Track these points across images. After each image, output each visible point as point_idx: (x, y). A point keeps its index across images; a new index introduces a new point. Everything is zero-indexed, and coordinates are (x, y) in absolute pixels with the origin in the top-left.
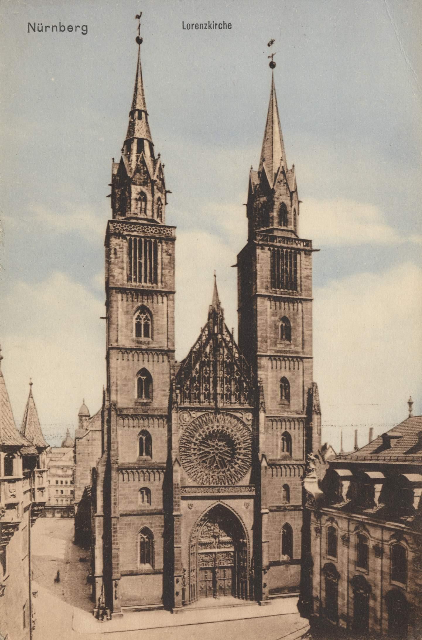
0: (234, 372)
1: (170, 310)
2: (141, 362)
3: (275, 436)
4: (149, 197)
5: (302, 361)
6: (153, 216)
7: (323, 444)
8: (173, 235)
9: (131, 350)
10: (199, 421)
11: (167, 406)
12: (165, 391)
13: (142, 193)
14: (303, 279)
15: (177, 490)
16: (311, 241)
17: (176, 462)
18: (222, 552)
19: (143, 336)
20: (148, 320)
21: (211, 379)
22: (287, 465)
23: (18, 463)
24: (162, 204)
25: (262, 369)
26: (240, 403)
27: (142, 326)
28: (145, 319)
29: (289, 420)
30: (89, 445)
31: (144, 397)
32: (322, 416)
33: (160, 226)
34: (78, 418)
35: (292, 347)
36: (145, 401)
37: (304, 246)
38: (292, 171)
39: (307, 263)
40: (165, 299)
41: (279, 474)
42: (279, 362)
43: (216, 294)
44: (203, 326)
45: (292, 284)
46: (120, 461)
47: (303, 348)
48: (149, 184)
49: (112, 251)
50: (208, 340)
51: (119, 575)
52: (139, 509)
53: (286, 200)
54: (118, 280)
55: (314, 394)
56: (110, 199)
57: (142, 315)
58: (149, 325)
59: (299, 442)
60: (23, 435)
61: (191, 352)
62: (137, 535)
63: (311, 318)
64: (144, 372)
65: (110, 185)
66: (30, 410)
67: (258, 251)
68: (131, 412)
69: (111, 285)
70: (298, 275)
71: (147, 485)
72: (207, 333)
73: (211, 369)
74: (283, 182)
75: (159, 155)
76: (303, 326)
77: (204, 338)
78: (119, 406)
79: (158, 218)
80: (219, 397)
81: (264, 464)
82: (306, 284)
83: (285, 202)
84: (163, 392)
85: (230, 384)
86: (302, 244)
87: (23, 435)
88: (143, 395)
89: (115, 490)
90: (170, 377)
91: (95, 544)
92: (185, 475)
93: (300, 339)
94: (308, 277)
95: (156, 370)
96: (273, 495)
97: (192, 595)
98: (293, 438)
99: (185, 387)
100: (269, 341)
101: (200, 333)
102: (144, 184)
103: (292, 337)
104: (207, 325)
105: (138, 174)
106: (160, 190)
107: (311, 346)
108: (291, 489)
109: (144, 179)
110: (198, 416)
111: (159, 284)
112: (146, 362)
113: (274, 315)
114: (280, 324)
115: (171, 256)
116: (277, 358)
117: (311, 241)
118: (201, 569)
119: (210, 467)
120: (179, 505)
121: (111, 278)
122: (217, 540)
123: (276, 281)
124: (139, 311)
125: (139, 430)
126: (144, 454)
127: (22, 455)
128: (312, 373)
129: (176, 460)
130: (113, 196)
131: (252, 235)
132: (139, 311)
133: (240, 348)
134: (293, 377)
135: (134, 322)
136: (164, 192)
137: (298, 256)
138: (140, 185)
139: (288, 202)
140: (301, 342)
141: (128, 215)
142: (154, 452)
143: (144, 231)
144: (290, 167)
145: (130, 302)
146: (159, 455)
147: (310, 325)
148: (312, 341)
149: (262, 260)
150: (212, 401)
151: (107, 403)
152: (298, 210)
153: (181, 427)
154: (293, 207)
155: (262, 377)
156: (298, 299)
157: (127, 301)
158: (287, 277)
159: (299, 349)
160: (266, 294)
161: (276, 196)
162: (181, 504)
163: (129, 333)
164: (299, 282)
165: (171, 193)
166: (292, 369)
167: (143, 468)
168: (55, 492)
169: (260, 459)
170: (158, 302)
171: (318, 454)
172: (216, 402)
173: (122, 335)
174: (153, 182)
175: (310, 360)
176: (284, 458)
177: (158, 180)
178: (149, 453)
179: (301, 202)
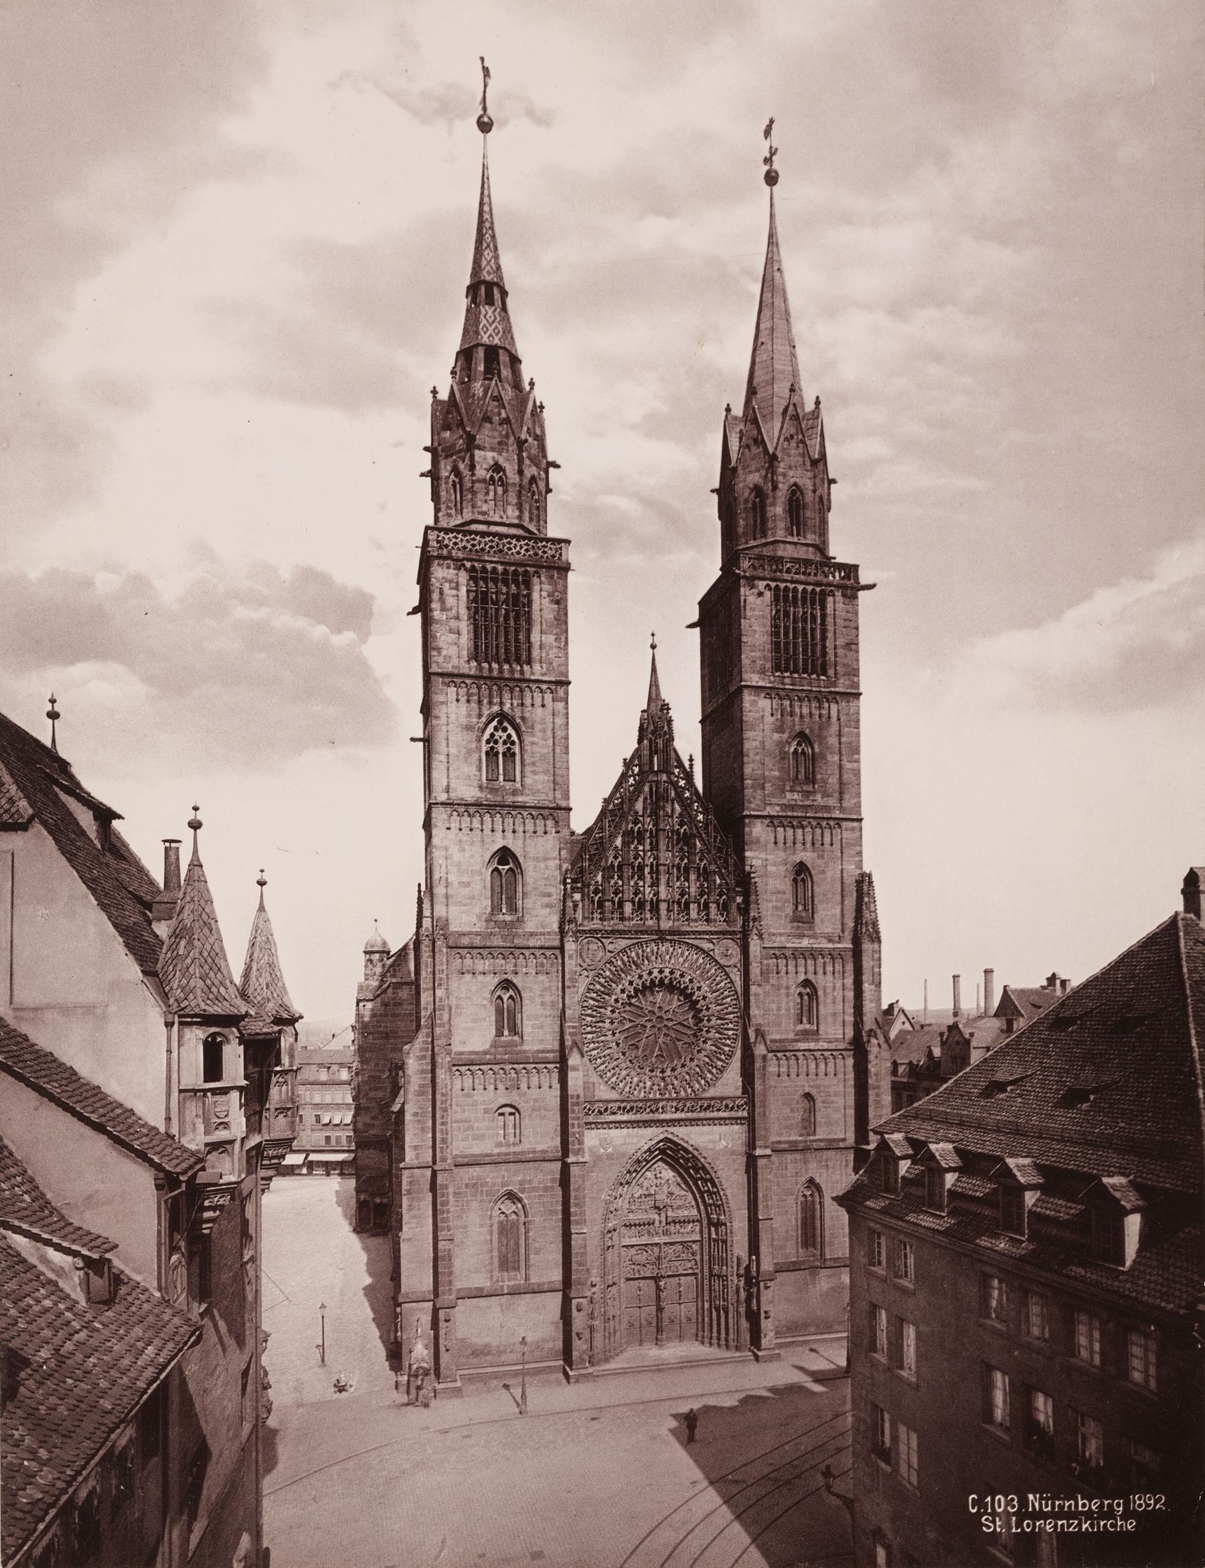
0: (695, 854)
2: (499, 834)
3: (783, 991)
5: (840, 827)
7: (885, 1006)
8: (564, 558)
9: (478, 804)
10: (622, 960)
11: (555, 927)
12: (550, 895)
13: (497, 468)
14: (839, 651)
15: (576, 1108)
16: (856, 567)
17: (575, 1050)
18: (672, 1244)
19: (501, 778)
20: (513, 743)
21: (647, 870)
22: (810, 1050)
23: (234, 1058)
24: (540, 493)
26: (707, 920)
27: (501, 756)
28: (505, 743)
29: (813, 954)
30: (386, 1015)
31: (504, 911)
32: (883, 944)
33: (538, 540)
34: (362, 958)
35: (819, 797)
36: (508, 918)
37: (842, 578)
38: (816, 414)
40: (548, 697)
41: (793, 1071)
42: (790, 832)
44: (628, 756)
45: (817, 664)
46: (457, 1047)
47: (841, 800)
48: (513, 447)
49: (435, 596)
51: (453, 1297)
52: (496, 1151)
54: (448, 658)
55: (866, 899)
58: (514, 754)
60: (243, 994)
61: (603, 814)
62: (492, 1208)
63: (858, 735)
64: (504, 855)
65: (426, 449)
66: (261, 943)
68: (477, 941)
69: (434, 668)
70: (829, 644)
71: (514, 1098)
72: (636, 770)
73: (648, 847)
74: (795, 440)
76: (840, 752)
78: (453, 928)
79: (531, 520)
80: (663, 907)
81: (760, 1050)
83: (800, 482)
84: (546, 900)
85: (687, 879)
86: (837, 574)
87: (243, 994)
88: (504, 906)
89: (445, 1110)
90: (560, 867)
91: (401, 1229)
92: (594, 1078)
93: (833, 780)
94: (852, 645)
95: (532, 851)
96: (780, 1121)
97: (609, 1335)
100: (767, 785)
101: (620, 769)
102: (501, 446)
103: (819, 777)
104: (637, 754)
105: (488, 425)
106: (535, 462)
107: (859, 795)
108: (819, 1104)
109: (501, 435)
110: (620, 948)
111: (537, 667)
113: (780, 729)
114: (792, 750)
115: (560, 602)
117: (856, 567)
118: (628, 1279)
119: (645, 1058)
120: (581, 1142)
121: (434, 653)
122: (663, 1218)
123: (782, 659)
124: (495, 723)
125: (496, 981)
126: (506, 1033)
127: (242, 1035)
128: (860, 853)
129: (575, 1043)
130: (433, 474)
131: (730, 557)
132: (495, 723)
134: (820, 862)
135: (485, 748)
136: (544, 465)
137: (830, 599)
138: (493, 449)
139: (806, 483)
140: (837, 787)
141: (468, 515)
143: (501, 551)
144: (809, 407)
145: (474, 705)
146: (538, 1032)
147: (857, 751)
148: (859, 784)
149: (753, 609)
150: (648, 915)
151: (427, 923)
152: (829, 501)
153: (586, 973)
154: (818, 493)
155: (754, 862)
156: (831, 692)
157: (468, 701)
159: (832, 802)
160: (761, 684)
161: (780, 470)
163: (473, 770)
164: (831, 656)
165: (558, 466)
166: (818, 844)
167: (506, 1059)
168: (314, 1119)
169: (752, 1040)
171: (874, 1027)
172: (658, 919)
174: (521, 444)
175: (856, 824)
177: (530, 440)
178: (514, 1030)
179: (834, 481)
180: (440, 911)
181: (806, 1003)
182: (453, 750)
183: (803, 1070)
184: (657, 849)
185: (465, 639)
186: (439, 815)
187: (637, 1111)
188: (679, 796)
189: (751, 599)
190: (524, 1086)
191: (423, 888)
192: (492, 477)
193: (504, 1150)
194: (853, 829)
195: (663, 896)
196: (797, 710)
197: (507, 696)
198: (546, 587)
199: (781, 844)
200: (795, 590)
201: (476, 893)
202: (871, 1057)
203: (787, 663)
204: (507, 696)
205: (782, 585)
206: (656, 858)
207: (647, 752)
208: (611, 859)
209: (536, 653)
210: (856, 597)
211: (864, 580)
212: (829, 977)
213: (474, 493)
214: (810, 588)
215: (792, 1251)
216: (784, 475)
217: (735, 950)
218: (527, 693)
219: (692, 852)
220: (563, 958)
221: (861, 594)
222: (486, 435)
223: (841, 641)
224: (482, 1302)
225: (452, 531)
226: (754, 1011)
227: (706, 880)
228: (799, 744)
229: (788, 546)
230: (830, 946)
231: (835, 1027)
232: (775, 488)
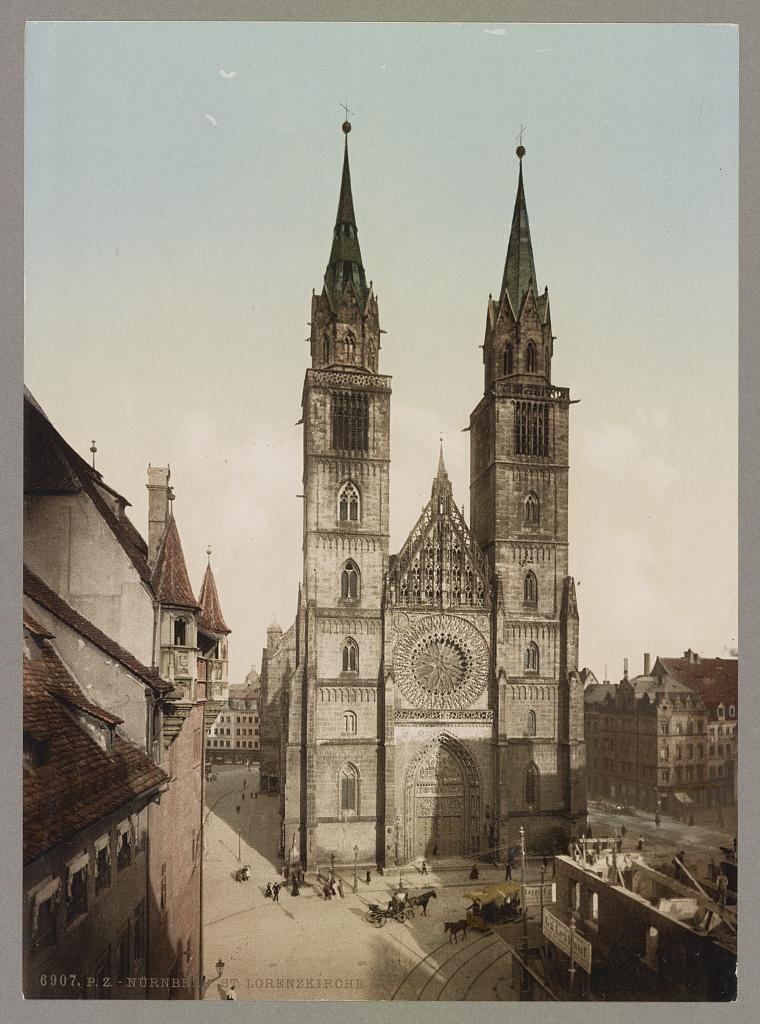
1: (383, 484)
4: (359, 340)
6: (363, 363)
9: (334, 532)
21: (435, 573)
25: (502, 560)
27: (349, 506)
29: (537, 625)
35: (542, 531)
36: (351, 601)
38: (545, 296)
39: (563, 420)
40: (378, 470)
43: (442, 464)
44: (425, 507)
46: (320, 676)
49: (312, 410)
50: (431, 522)
53: (537, 337)
56: (309, 342)
57: (349, 491)
59: (549, 655)
64: (350, 564)
67: (498, 406)
72: (430, 513)
73: (436, 560)
75: (371, 283)
77: (426, 520)
78: (319, 606)
80: (444, 595)
81: (502, 682)
82: (561, 447)
83: (532, 337)
85: (459, 580)
92: (400, 696)
93: (551, 521)
94: (565, 438)
98: (540, 650)
99: (402, 584)
102: (351, 321)
111: (371, 452)
112: (353, 550)
113: (518, 489)
115: (386, 414)
116: (521, 546)
123: (521, 446)
124: (346, 485)
128: (566, 565)
130: (313, 340)
131: (490, 385)
132: (346, 485)
133: (473, 533)
135: (339, 500)
137: (552, 410)
141: (332, 363)
142: (361, 667)
144: (541, 292)
145: (334, 475)
146: (368, 668)
149: (502, 417)
153: (396, 634)
157: (330, 472)
158: (535, 438)
161: (522, 331)
162: (396, 733)
163: (332, 513)
166: (540, 559)
170: (368, 474)
172: (442, 603)
173: (323, 517)
176: (530, 675)
178: (354, 667)
180: (312, 596)
181: (531, 656)
182: (321, 501)
183: (528, 696)
184: (442, 561)
185: (329, 436)
186: (312, 539)
187: (430, 717)
188: (456, 529)
189: (502, 410)
190: (359, 699)
191: (302, 582)
192: (347, 339)
193: (346, 737)
194: (564, 550)
195: (444, 589)
196: (529, 477)
197: (353, 467)
198: (378, 404)
199: (517, 559)
200: (530, 404)
201: (333, 585)
202: (571, 689)
203: (524, 450)
204: (353, 467)
205: (521, 401)
206: (441, 566)
207: (436, 503)
208: (413, 566)
209: (370, 443)
210: (568, 408)
211: (571, 399)
212: (546, 640)
213: (335, 348)
214: (538, 403)
215: (520, 803)
216: (524, 334)
217: (487, 623)
218: (365, 466)
219: (462, 563)
220: (383, 624)
221: (571, 405)
222: (343, 312)
223: (558, 435)
224: (333, 826)
225: (322, 371)
226: (500, 659)
227: (471, 580)
228: (530, 498)
229: (525, 378)
230: (547, 621)
231: (549, 668)
232: (518, 342)
